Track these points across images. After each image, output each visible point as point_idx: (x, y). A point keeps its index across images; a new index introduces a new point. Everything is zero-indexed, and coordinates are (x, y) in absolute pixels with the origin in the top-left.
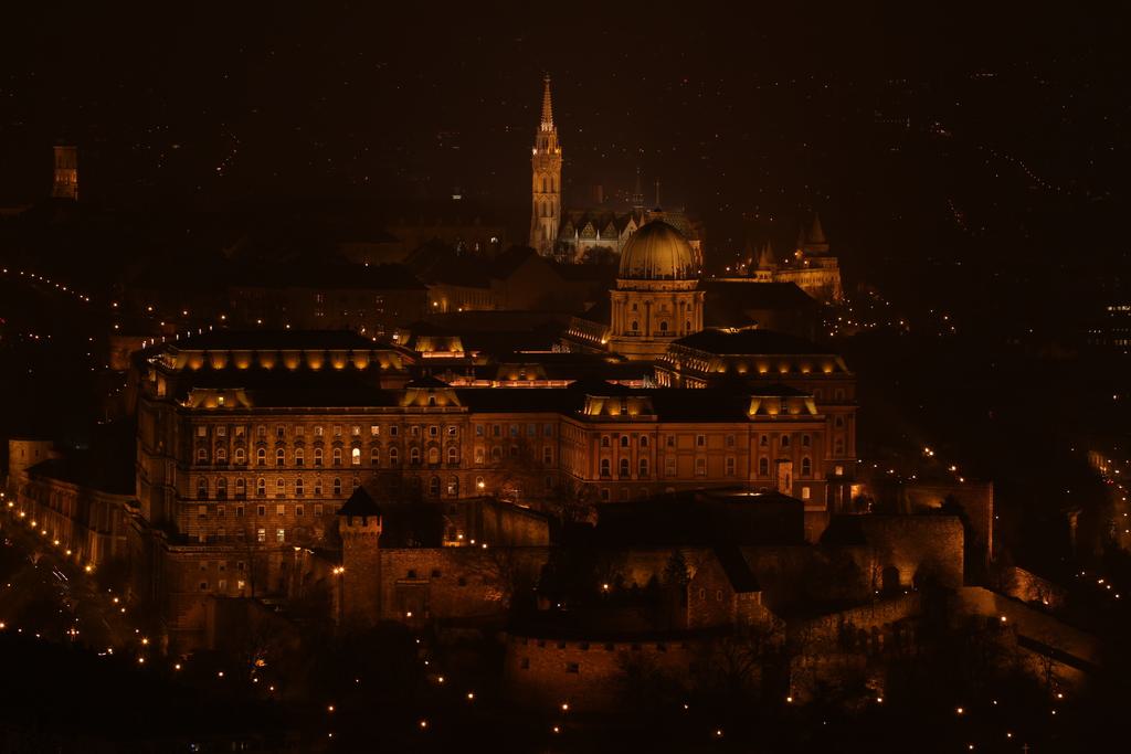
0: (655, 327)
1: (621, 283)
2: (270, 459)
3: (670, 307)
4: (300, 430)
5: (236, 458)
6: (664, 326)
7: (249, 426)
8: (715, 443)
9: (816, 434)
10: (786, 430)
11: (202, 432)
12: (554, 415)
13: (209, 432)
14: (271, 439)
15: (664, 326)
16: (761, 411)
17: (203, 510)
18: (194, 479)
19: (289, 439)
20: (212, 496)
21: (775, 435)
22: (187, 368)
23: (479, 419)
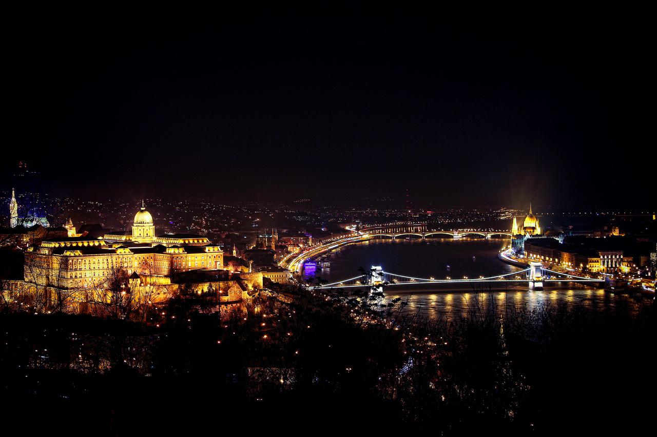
0: (145, 235)
1: (135, 225)
2: (87, 268)
3: (148, 230)
4: (94, 260)
5: (79, 268)
6: (147, 234)
7: (82, 260)
8: (199, 258)
9: (221, 255)
10: (215, 254)
11: (71, 261)
12: (153, 254)
13: (72, 261)
14: (87, 262)
15: (147, 234)
16: (209, 250)
17: (71, 281)
18: (69, 273)
19: (92, 262)
20: (74, 277)
21: (212, 256)
22: (94, 245)
23: (136, 255)
